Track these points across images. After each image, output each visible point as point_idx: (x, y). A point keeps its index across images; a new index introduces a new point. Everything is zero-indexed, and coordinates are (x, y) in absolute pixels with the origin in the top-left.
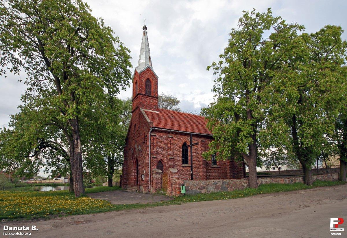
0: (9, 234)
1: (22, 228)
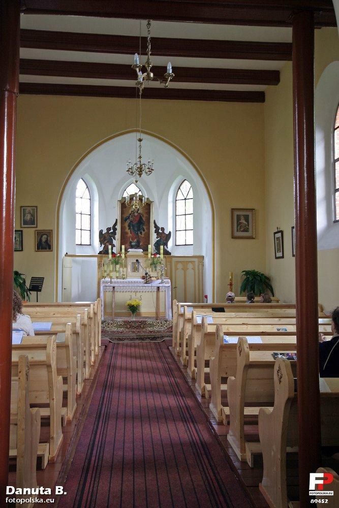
0: (15, 501)
1: (39, 491)
